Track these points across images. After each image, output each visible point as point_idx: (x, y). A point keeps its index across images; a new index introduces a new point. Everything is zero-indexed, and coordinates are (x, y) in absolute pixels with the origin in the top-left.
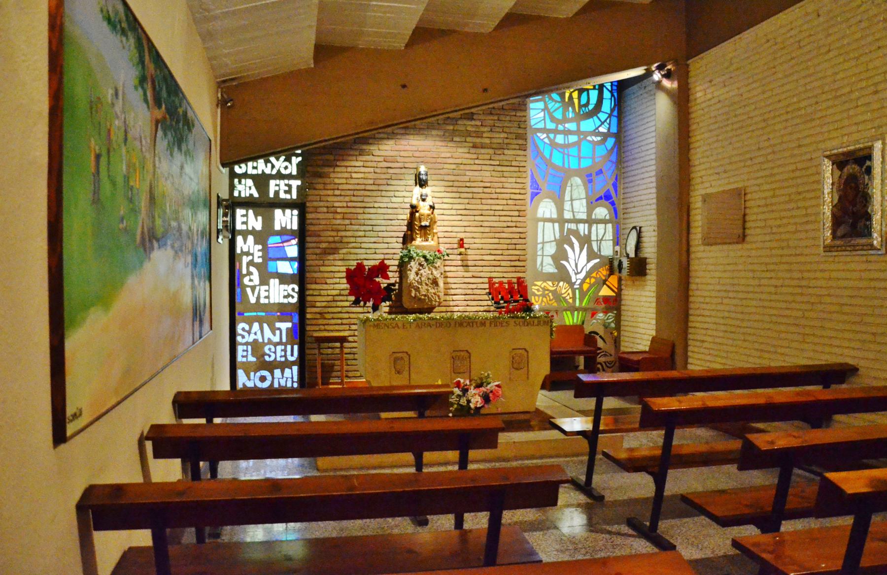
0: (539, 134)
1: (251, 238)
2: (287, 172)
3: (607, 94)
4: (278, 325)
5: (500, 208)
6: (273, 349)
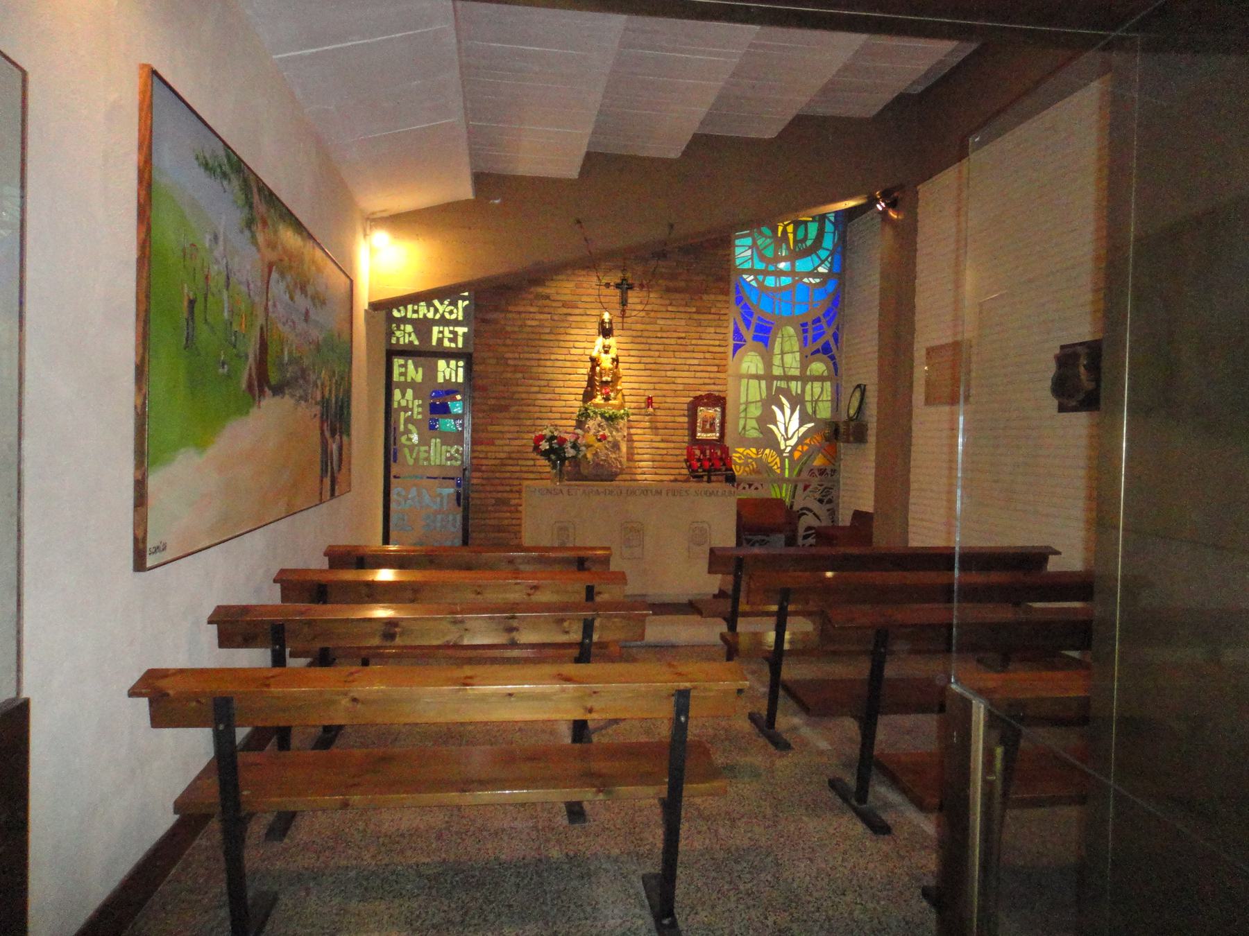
1: (410, 393)
2: (453, 317)
3: (829, 227)
5: (696, 362)
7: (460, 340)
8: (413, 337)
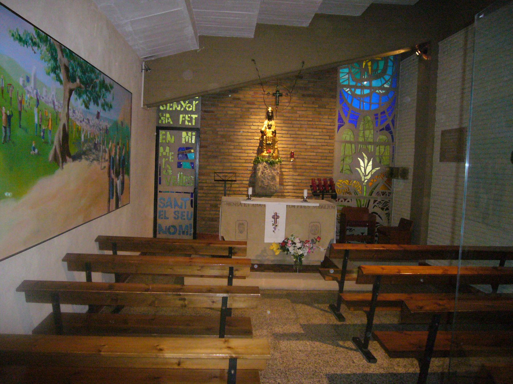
0: (345, 89)
1: (168, 148)
2: (191, 109)
3: (390, 64)
5: (318, 134)
7: (194, 121)
8: (170, 120)
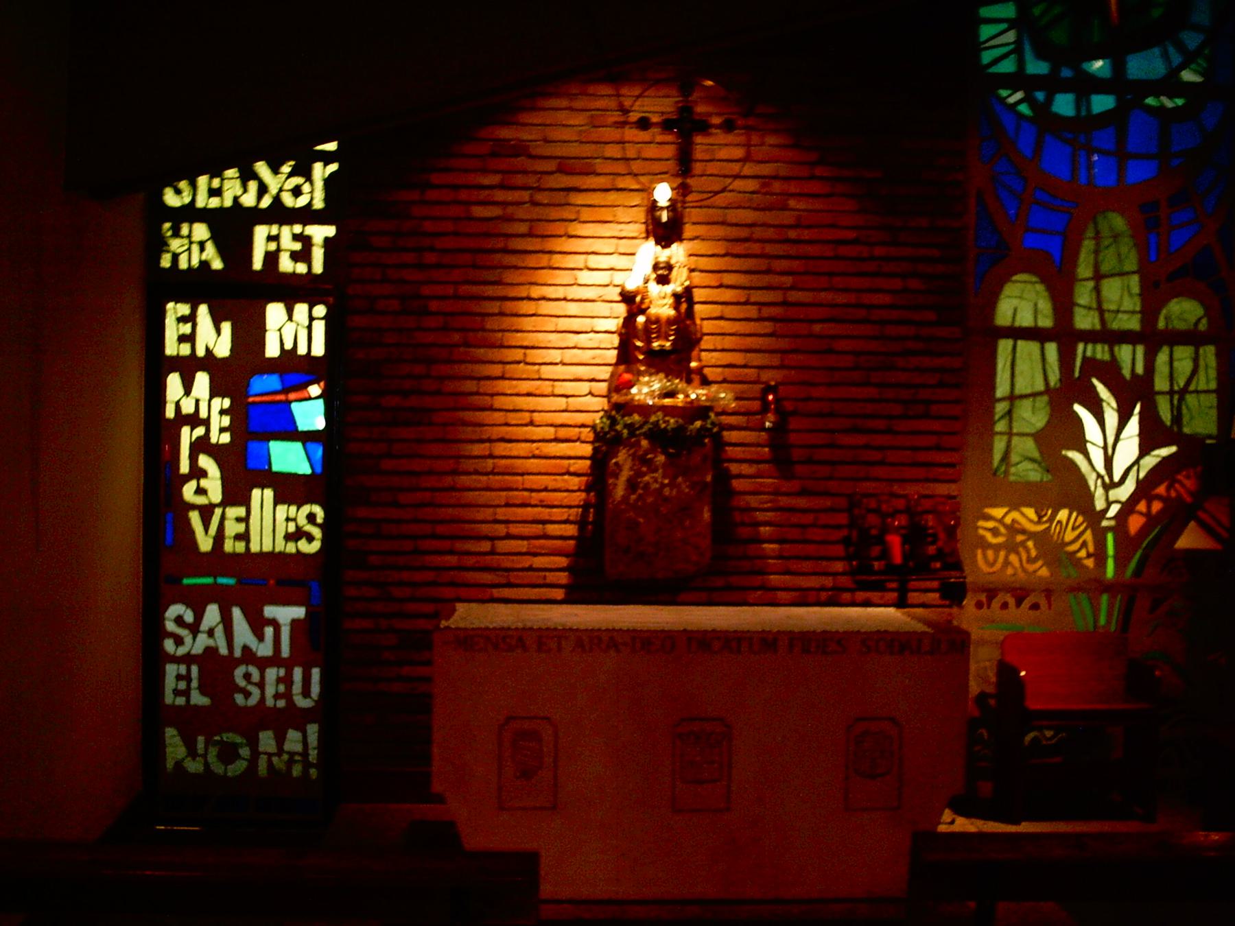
0: (1004, 93)
1: (202, 380)
2: (302, 202)
4: (270, 611)
5: (886, 299)
6: (256, 676)
7: (318, 255)
8: (210, 252)
